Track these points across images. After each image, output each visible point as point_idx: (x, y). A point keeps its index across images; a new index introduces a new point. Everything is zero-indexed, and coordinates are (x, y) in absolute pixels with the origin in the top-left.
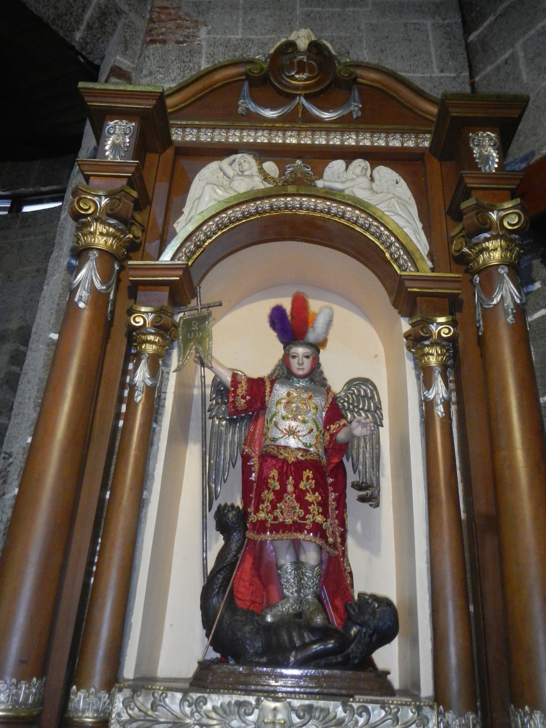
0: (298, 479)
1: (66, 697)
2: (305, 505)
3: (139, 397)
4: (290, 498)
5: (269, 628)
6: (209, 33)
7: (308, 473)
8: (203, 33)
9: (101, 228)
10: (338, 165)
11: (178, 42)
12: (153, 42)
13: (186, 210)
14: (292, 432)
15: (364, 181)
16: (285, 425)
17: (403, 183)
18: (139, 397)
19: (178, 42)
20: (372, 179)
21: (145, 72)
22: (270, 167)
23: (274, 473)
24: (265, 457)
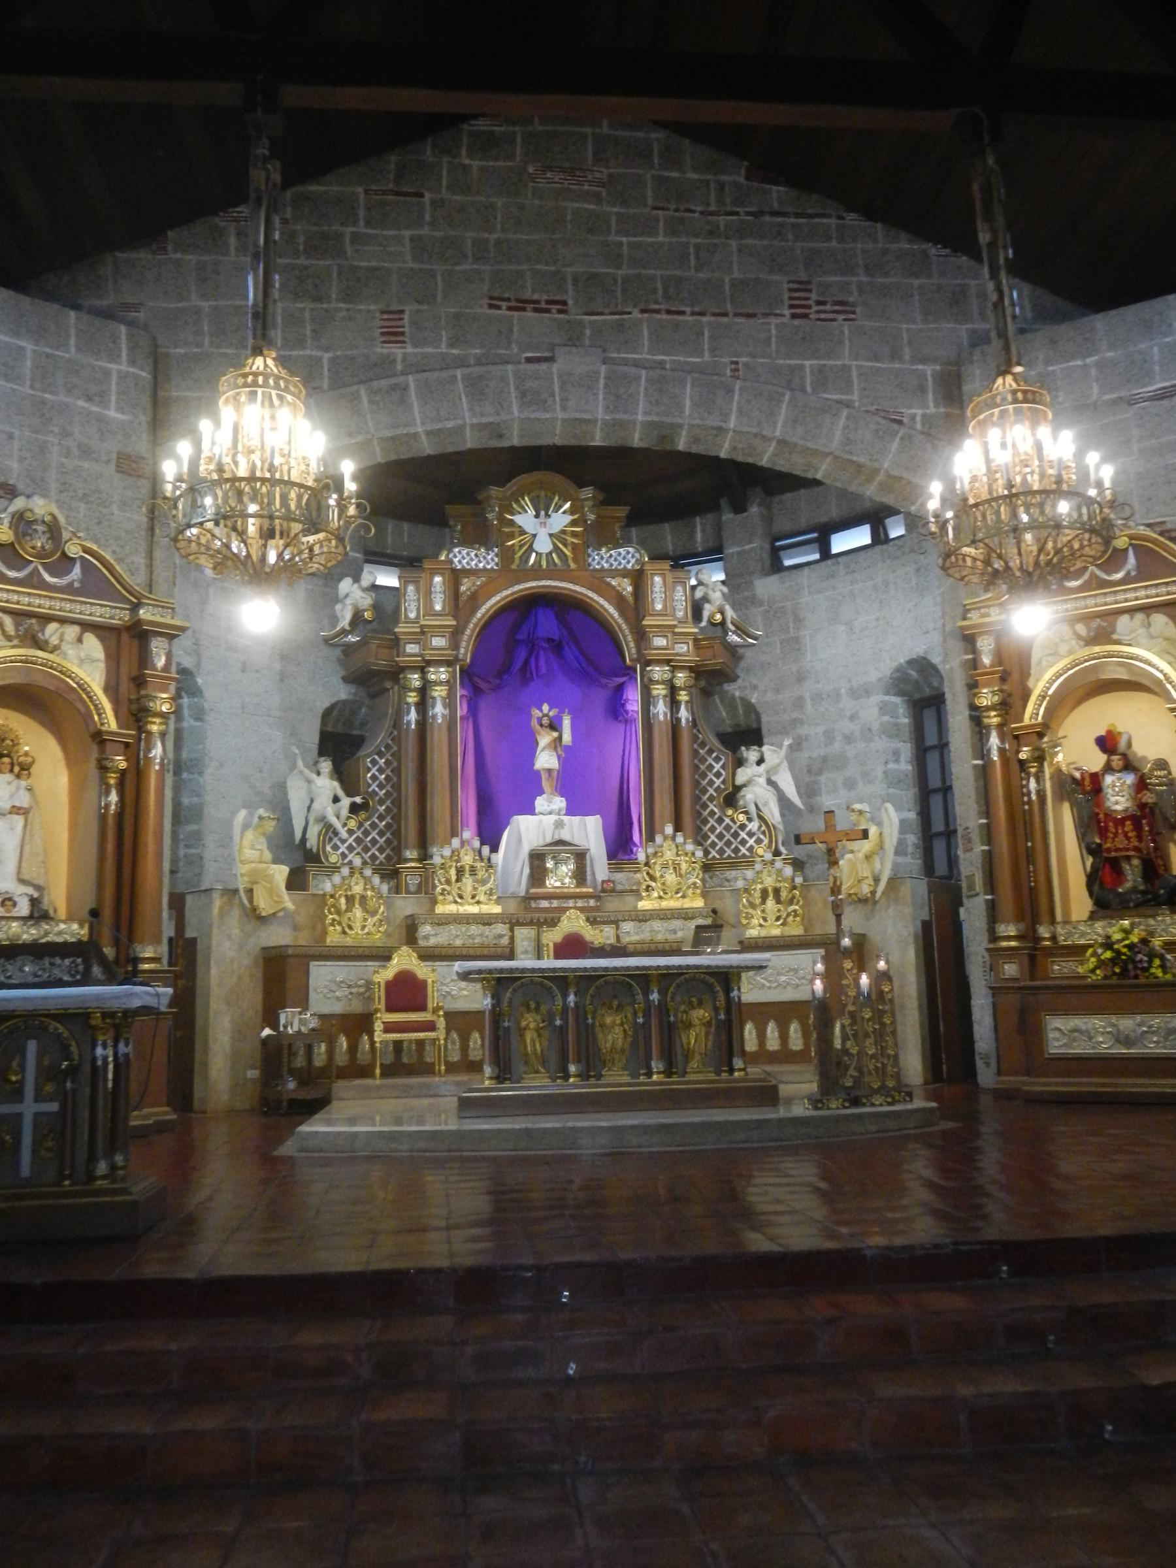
0: (1123, 826)
1: (1035, 931)
2: (1128, 838)
3: (1034, 797)
4: (1121, 837)
5: (1120, 894)
7: (1128, 823)
9: (993, 713)
10: (1124, 620)
13: (1033, 672)
14: (1117, 803)
16: (1113, 799)
17: (1171, 623)
18: (1034, 797)
20: (1149, 624)
23: (1111, 824)
24: (1106, 815)
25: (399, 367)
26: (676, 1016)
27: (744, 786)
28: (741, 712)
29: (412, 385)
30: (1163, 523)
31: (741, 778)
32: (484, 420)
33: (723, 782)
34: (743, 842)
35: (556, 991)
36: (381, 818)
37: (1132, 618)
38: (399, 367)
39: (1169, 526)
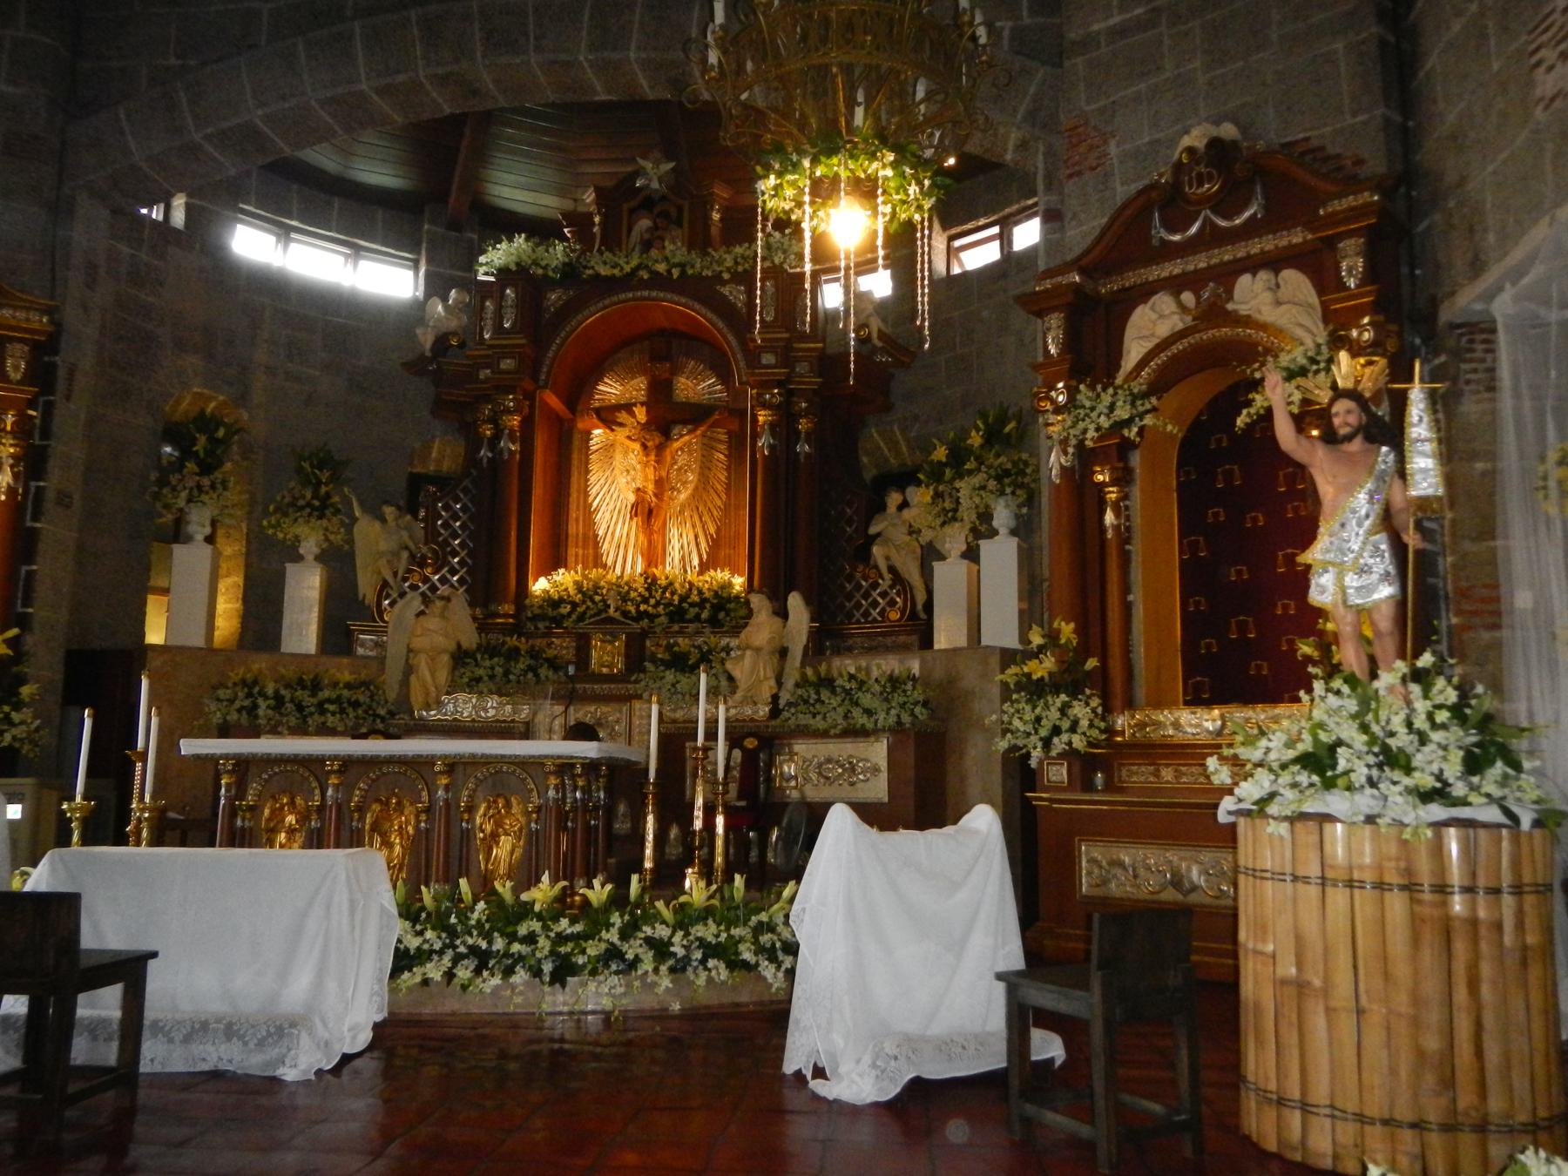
6: (1118, 146)
8: (1113, 149)
10: (1244, 280)
11: (1093, 169)
12: (1070, 176)
15: (1267, 297)
19: (1093, 169)
20: (1278, 286)
21: (1069, 215)
22: (1188, 297)
25: (349, 13)
26: (471, 820)
27: (879, 535)
28: (904, 449)
29: (358, 30)
30: (1307, 139)
31: (873, 530)
32: (440, 71)
33: (856, 530)
34: (875, 604)
35: (315, 784)
36: (453, 572)
37: (1254, 275)
38: (349, 13)
39: (1315, 143)
